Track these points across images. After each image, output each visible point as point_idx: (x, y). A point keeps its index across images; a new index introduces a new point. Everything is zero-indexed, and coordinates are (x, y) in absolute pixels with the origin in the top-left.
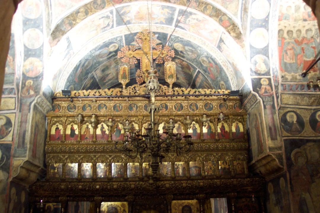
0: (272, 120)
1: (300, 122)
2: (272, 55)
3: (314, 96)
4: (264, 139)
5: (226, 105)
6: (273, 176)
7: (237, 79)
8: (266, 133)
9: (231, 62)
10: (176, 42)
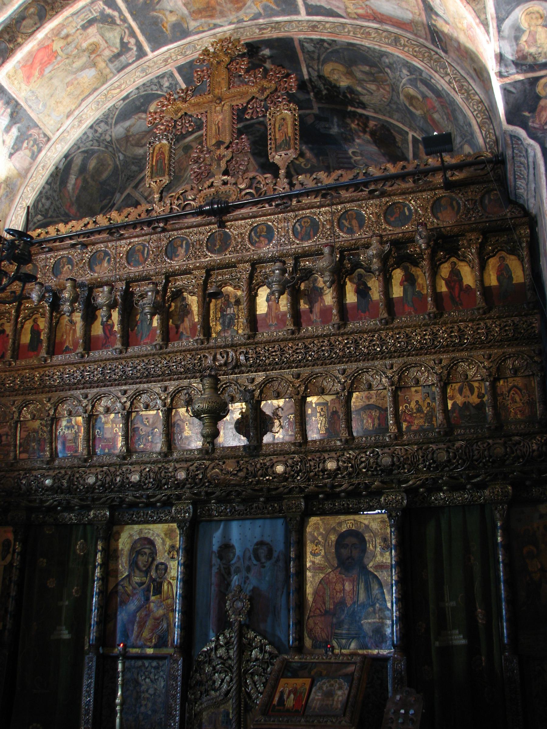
5: (454, 203)
10: (324, 62)
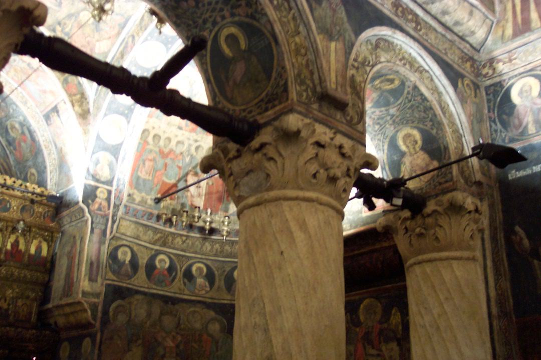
0: (97, 252)
1: (134, 264)
2: (124, 159)
3: (161, 233)
4: (79, 276)
5: (32, 210)
6: (74, 333)
7: (60, 174)
8: (83, 269)
9: (59, 145)
